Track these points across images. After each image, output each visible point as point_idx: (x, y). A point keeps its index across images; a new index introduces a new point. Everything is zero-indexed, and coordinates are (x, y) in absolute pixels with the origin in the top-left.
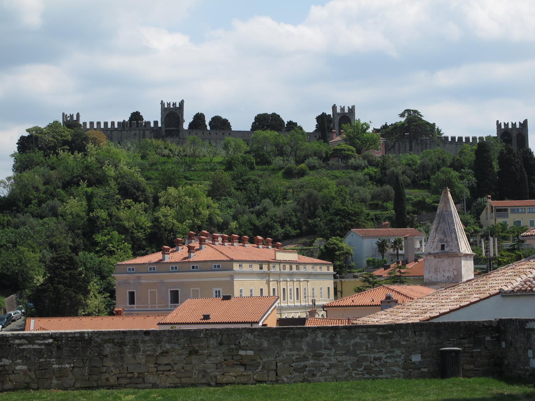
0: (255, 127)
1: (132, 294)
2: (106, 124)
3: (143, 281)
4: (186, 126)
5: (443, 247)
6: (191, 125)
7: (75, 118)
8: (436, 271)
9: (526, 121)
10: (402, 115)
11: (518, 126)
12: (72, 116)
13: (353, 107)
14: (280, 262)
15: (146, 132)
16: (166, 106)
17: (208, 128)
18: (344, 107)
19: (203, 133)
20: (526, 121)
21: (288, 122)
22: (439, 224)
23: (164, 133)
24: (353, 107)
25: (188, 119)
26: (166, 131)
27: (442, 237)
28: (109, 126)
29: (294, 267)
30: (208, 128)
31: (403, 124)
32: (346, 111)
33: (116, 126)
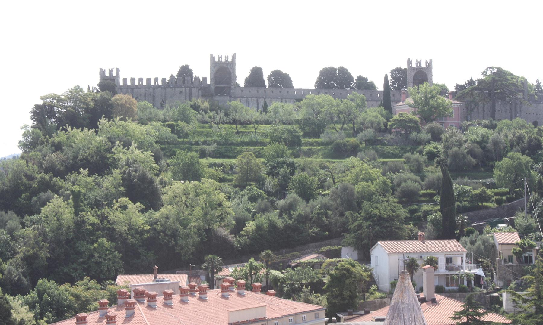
2: (149, 80)
12: (111, 71)
15: (193, 89)
18: (421, 61)
19: (258, 91)
21: (357, 77)
24: (431, 61)
26: (216, 88)
32: (423, 65)
33: (160, 83)
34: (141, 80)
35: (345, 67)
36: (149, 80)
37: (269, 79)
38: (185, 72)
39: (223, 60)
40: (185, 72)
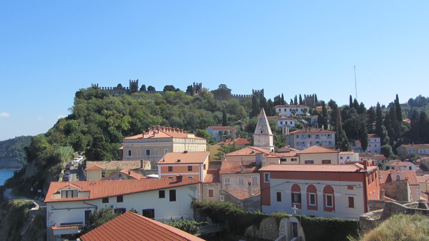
1: (130, 152)
2: (108, 88)
3: (134, 146)
4: (139, 89)
5: (262, 132)
6: (141, 89)
7: (96, 86)
8: (259, 142)
9: (263, 90)
10: (220, 86)
11: (260, 91)
12: (95, 85)
13: (201, 83)
14: (189, 138)
15: (124, 91)
16: (131, 82)
17: (147, 90)
18: (198, 83)
20: (263, 90)
22: (260, 122)
24: (201, 83)
25: (140, 86)
28: (110, 89)
29: (194, 140)
30: (147, 90)
32: (198, 85)
33: (112, 89)
36: (108, 88)
37: (148, 88)
38: (120, 85)
40: (120, 85)
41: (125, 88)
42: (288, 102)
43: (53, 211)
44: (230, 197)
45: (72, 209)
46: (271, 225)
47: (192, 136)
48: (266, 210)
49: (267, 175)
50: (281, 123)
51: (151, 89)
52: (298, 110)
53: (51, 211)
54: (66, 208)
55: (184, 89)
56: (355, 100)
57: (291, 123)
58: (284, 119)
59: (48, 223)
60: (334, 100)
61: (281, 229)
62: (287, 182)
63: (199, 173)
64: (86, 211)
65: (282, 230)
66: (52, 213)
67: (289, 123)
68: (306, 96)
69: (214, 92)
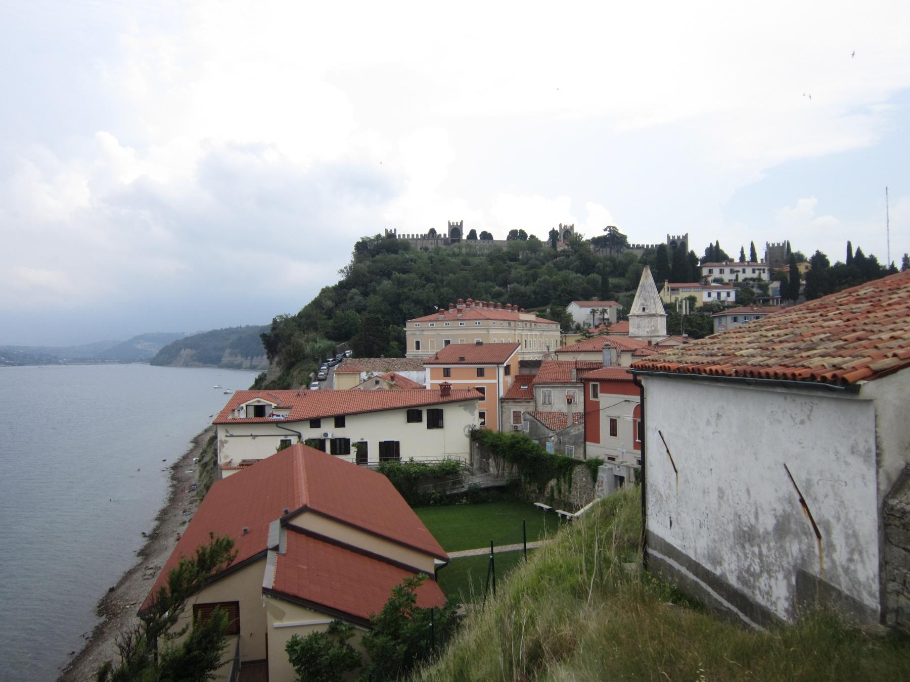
0: (508, 238)
1: (418, 343)
2: (413, 235)
4: (464, 237)
5: (644, 309)
9: (687, 235)
10: (605, 230)
11: (681, 238)
12: (391, 231)
14: (523, 321)
17: (479, 238)
20: (687, 235)
22: (641, 292)
23: (450, 242)
24: (573, 225)
26: (452, 240)
27: (643, 302)
28: (415, 237)
29: (533, 324)
30: (479, 238)
31: (605, 237)
33: (419, 237)
34: (408, 235)
35: (523, 229)
36: (413, 235)
38: (432, 231)
39: (455, 224)
40: (432, 231)
41: (440, 235)
42: (735, 256)
43: (227, 439)
44: (537, 425)
45: (259, 437)
46: (584, 480)
47: (532, 317)
48: (593, 451)
49: (595, 387)
50: (709, 295)
51: (486, 236)
52: (746, 271)
53: (224, 438)
54: (249, 434)
55: (544, 237)
56: (859, 252)
57: (728, 295)
58: (716, 288)
59: (220, 459)
60: (824, 251)
61: (598, 487)
62: (626, 401)
63: (496, 381)
64: (282, 441)
65: (600, 488)
66: (226, 442)
67: (723, 295)
68: (771, 246)
69: (597, 241)
